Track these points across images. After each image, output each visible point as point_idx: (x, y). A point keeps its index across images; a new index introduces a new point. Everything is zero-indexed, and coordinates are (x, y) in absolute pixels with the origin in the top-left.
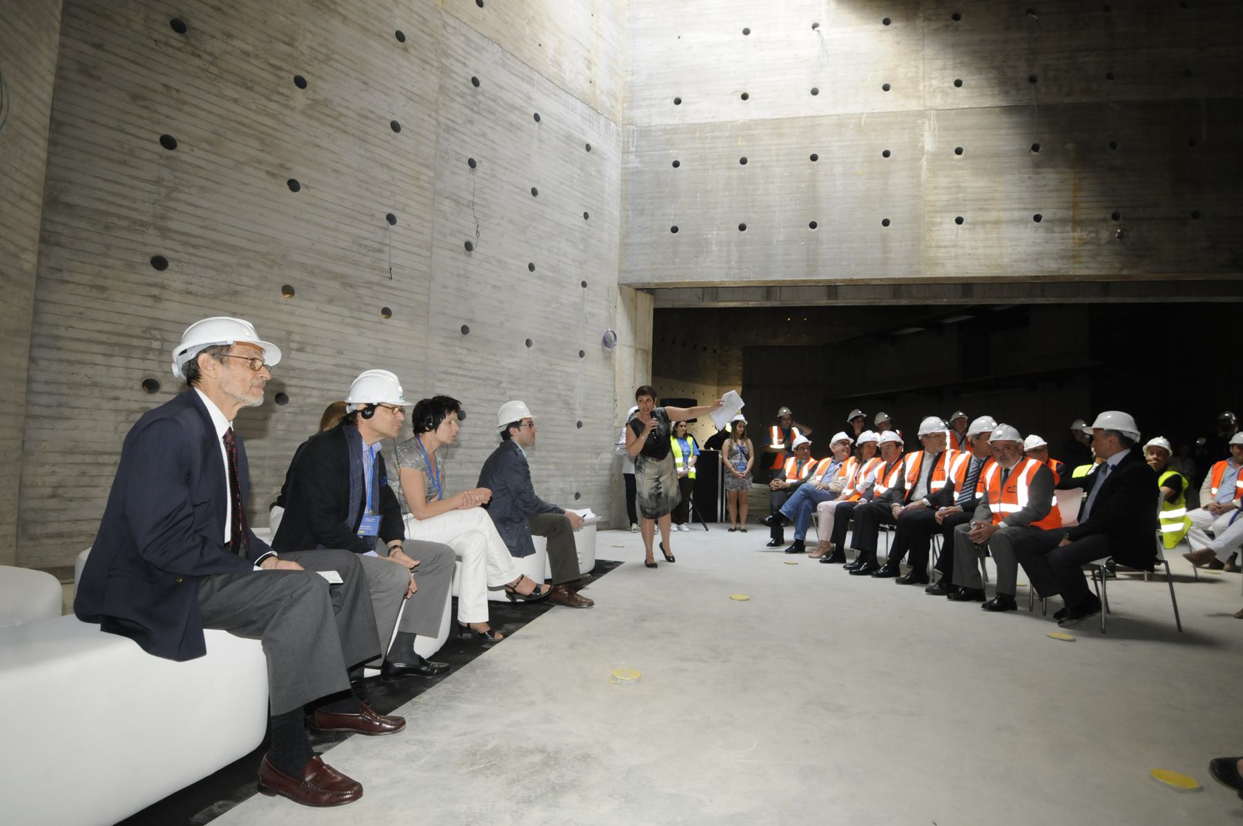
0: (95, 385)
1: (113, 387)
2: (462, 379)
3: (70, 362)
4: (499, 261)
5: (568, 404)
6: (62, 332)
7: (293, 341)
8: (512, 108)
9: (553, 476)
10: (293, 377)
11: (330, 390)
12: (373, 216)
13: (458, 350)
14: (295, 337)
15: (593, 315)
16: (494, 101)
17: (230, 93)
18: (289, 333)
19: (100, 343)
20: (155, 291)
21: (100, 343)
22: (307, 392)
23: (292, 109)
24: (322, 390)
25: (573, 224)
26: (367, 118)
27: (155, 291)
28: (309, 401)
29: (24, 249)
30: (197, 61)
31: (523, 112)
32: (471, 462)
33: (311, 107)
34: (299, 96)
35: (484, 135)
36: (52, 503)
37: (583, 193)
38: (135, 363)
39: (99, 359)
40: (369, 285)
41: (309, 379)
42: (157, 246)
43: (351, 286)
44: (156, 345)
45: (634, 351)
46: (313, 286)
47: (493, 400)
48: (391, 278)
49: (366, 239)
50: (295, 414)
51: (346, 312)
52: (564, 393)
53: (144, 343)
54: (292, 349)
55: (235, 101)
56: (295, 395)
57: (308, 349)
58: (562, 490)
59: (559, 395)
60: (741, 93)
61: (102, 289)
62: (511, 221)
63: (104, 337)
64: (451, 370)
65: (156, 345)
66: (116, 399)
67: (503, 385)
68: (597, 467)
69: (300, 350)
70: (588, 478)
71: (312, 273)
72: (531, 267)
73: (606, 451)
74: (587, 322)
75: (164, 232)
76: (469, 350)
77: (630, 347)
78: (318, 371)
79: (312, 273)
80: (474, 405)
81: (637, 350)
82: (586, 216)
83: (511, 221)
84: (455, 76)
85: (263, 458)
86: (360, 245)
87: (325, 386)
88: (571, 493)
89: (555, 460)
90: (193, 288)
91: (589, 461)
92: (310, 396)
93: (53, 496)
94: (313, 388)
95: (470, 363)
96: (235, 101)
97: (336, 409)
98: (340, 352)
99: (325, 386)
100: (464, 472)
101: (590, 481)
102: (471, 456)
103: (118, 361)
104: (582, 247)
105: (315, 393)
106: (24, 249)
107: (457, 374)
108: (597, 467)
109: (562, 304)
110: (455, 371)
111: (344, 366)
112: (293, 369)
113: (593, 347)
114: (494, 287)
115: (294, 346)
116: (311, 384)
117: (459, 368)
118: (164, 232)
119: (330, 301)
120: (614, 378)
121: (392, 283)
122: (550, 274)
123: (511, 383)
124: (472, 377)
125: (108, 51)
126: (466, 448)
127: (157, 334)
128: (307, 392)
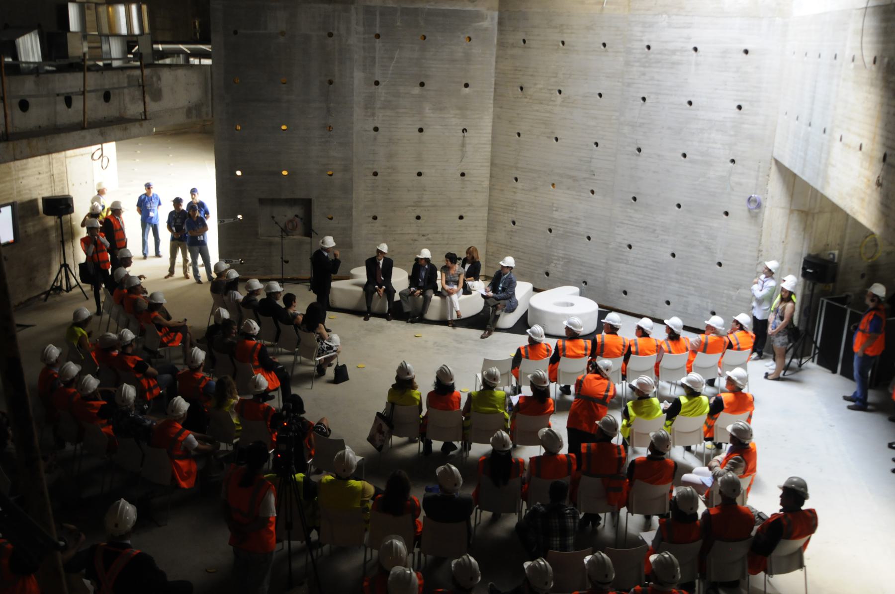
4: (659, 156)
5: (710, 249)
7: (555, 207)
8: (674, 52)
12: (587, 145)
14: (555, 205)
15: (740, 184)
16: (660, 54)
18: (553, 203)
19: (502, 208)
20: (514, 190)
21: (502, 208)
22: (558, 228)
23: (556, 105)
24: (564, 228)
25: (725, 118)
26: (587, 97)
27: (514, 190)
28: (559, 232)
29: (483, 181)
30: (526, 100)
31: (682, 50)
32: (633, 273)
33: (563, 102)
34: (559, 98)
35: (652, 79)
38: (510, 215)
40: (584, 179)
42: (418, 213)
44: (514, 209)
45: (788, 211)
48: (594, 175)
52: (706, 240)
55: (537, 111)
58: (698, 305)
59: (701, 242)
61: (502, 190)
62: (669, 128)
65: (514, 209)
66: (505, 227)
68: (734, 298)
69: (556, 211)
70: (725, 304)
72: (684, 155)
73: (745, 288)
75: (517, 168)
77: (783, 208)
78: (563, 220)
80: (637, 242)
81: (792, 211)
82: (740, 107)
83: (669, 128)
84: (634, 51)
87: (565, 226)
88: (707, 310)
89: (695, 285)
91: (726, 292)
92: (559, 230)
93: (492, 255)
94: (561, 227)
96: (537, 111)
97: (417, 259)
98: (571, 212)
99: (565, 226)
100: (629, 278)
101: (726, 306)
103: (506, 214)
104: (732, 133)
105: (562, 229)
106: (483, 181)
107: (627, 224)
108: (734, 298)
112: (554, 218)
113: (739, 208)
114: (654, 172)
115: (554, 209)
117: (629, 220)
118: (517, 168)
119: (568, 189)
123: (663, 231)
124: (636, 226)
126: (631, 265)
127: (514, 205)
128: (558, 228)
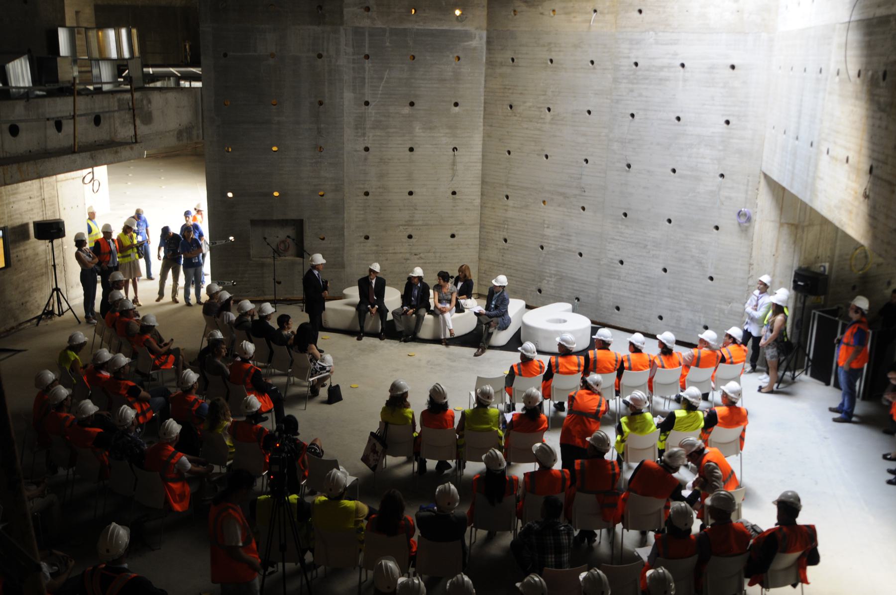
0: (493, 240)
1: (497, 241)
2: (622, 242)
3: (487, 232)
4: (649, 171)
5: (701, 263)
6: (485, 223)
8: (661, 68)
9: (683, 309)
10: (545, 239)
11: (558, 245)
12: (577, 162)
13: (620, 226)
14: (546, 222)
15: (730, 198)
16: (648, 70)
17: (525, 126)
18: (544, 220)
20: (506, 208)
22: (550, 245)
23: (544, 123)
24: (555, 245)
25: (713, 133)
26: (575, 114)
27: (506, 208)
28: (551, 249)
29: (474, 200)
30: (516, 118)
31: (670, 67)
32: (625, 289)
33: (552, 119)
34: (548, 116)
35: (640, 95)
36: (484, 275)
37: (725, 106)
38: (501, 233)
39: (493, 231)
40: (575, 196)
41: (551, 240)
42: (410, 231)
43: (568, 198)
44: (506, 226)
45: (778, 225)
46: (552, 199)
47: (641, 256)
48: (585, 191)
49: (574, 174)
50: (546, 254)
51: (565, 210)
52: (697, 255)
53: (503, 226)
54: (545, 227)
55: (527, 129)
56: (547, 246)
57: (551, 227)
58: (691, 320)
59: (692, 257)
60: (453, 191)
61: (494, 208)
62: (658, 144)
63: (494, 224)
64: (616, 238)
67: (649, 247)
68: (726, 312)
69: (548, 227)
70: (717, 318)
71: (552, 194)
72: (674, 171)
73: (737, 302)
74: (723, 204)
75: (508, 186)
76: (627, 226)
77: (773, 221)
78: (554, 237)
79: (552, 194)
80: (629, 257)
81: (781, 225)
82: (728, 122)
83: (658, 144)
84: (622, 68)
85: (535, 271)
86: (571, 177)
88: (700, 324)
89: (687, 299)
90: (516, 205)
91: (718, 306)
92: (551, 247)
93: (484, 273)
94: (552, 244)
95: (627, 233)
96: (527, 129)
98: (563, 228)
100: (621, 293)
101: (719, 320)
102: (626, 286)
103: (497, 232)
104: (721, 148)
105: (553, 246)
106: (474, 200)
107: (618, 240)
108: (726, 312)
109: (699, 193)
110: (618, 238)
111: (564, 234)
112: (545, 235)
113: (729, 222)
114: (644, 188)
115: (546, 226)
116: (551, 242)
117: (620, 236)
118: (508, 186)
119: (559, 206)
120: (751, 247)
121: (586, 194)
122: (689, 173)
123: (654, 246)
124: (628, 242)
125: (494, 126)
126: (623, 280)
127: (506, 222)
128: (550, 245)
